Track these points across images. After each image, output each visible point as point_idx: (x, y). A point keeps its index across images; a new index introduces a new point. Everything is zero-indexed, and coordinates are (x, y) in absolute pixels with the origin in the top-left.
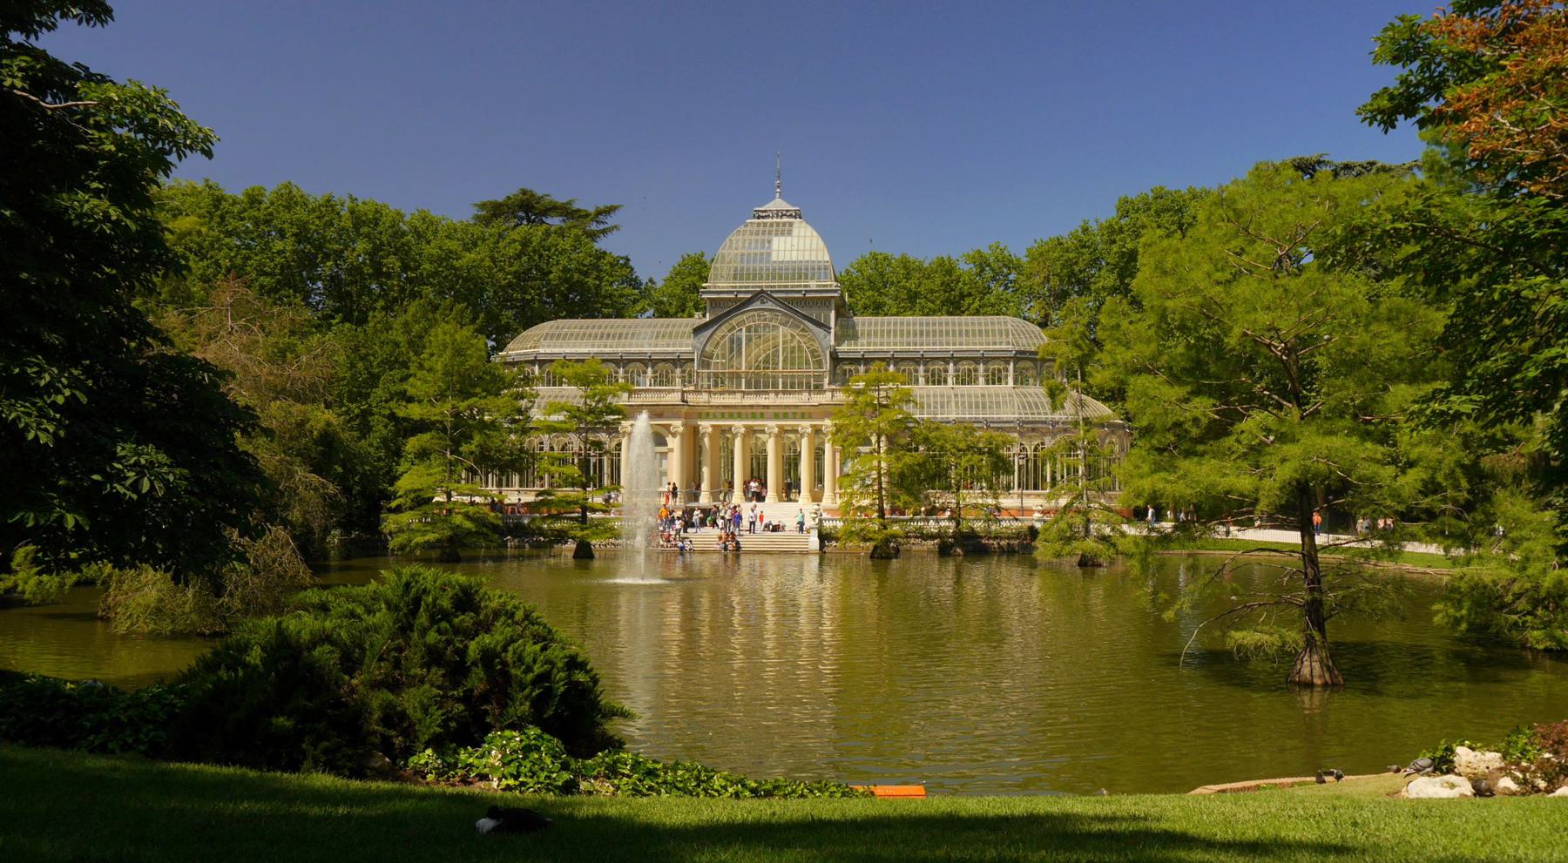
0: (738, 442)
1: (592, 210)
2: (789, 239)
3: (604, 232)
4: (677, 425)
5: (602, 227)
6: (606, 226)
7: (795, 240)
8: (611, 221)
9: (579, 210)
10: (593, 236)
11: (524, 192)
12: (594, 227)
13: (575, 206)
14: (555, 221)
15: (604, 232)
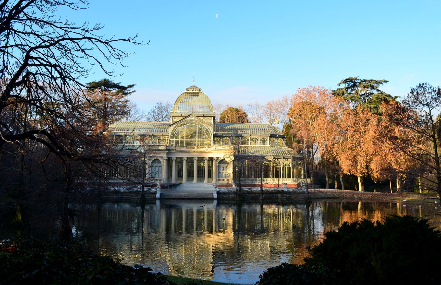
0: (184, 162)
1: (126, 86)
2: (198, 98)
3: (129, 93)
4: (165, 156)
5: (129, 92)
6: (130, 91)
7: (200, 98)
8: (132, 89)
9: (122, 86)
10: (126, 94)
11: (104, 79)
12: (126, 91)
13: (121, 85)
14: (114, 91)
15: (129, 93)
